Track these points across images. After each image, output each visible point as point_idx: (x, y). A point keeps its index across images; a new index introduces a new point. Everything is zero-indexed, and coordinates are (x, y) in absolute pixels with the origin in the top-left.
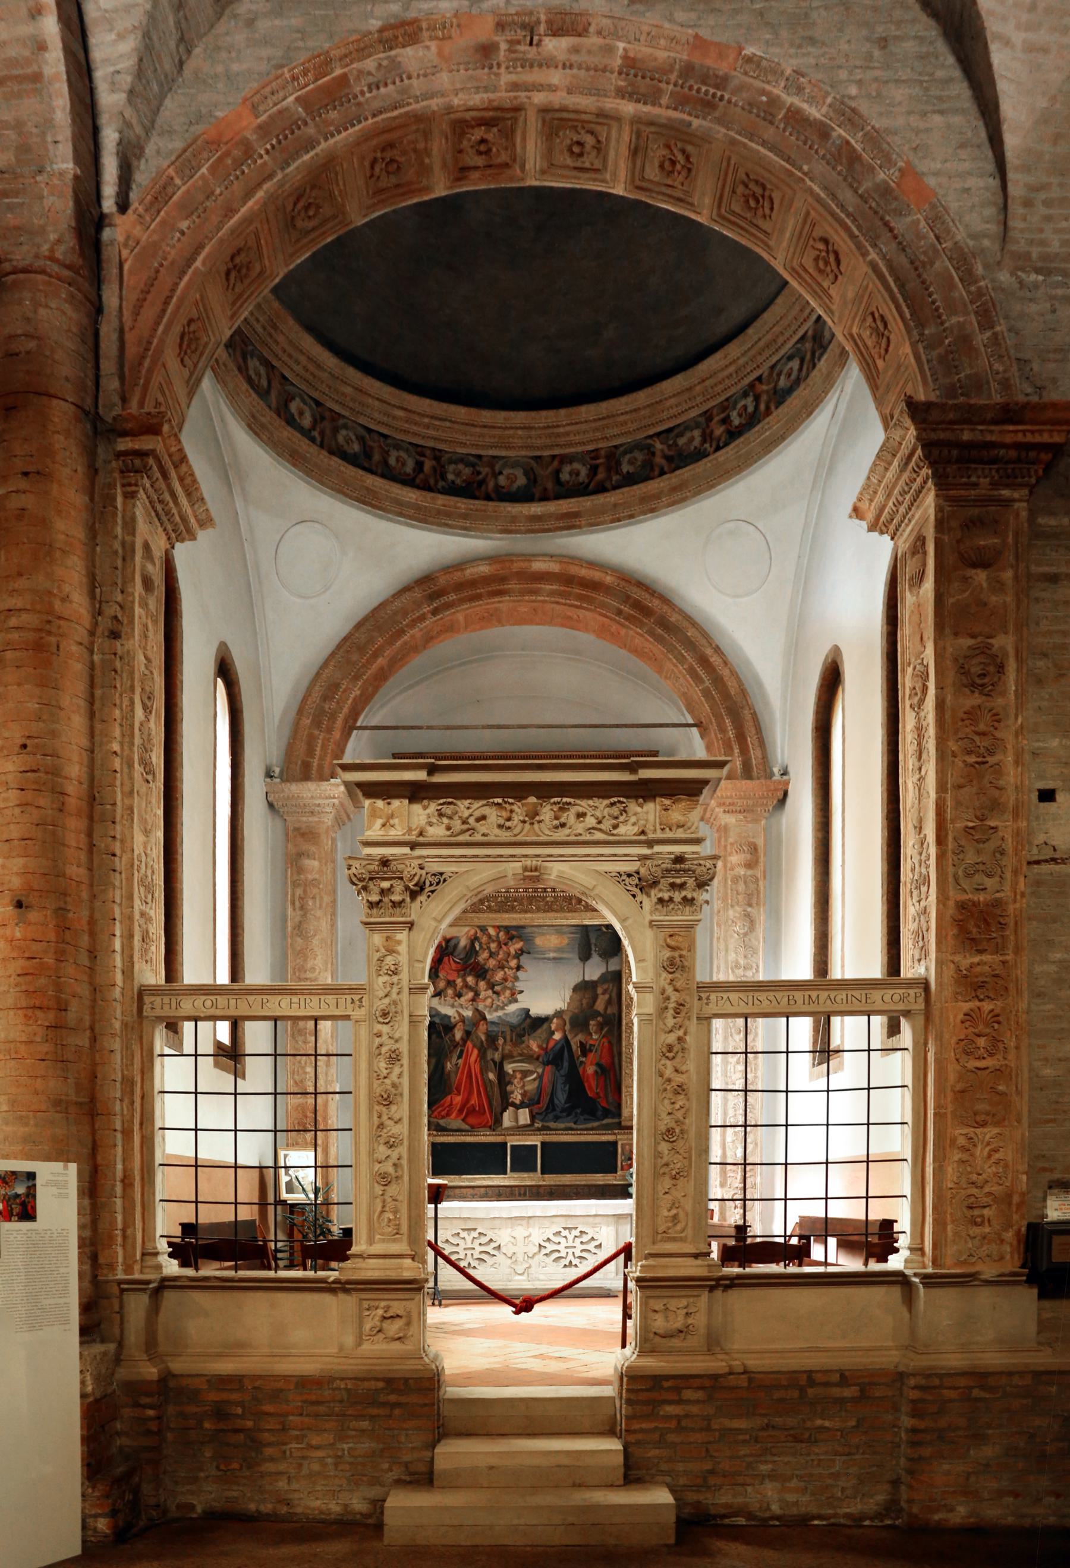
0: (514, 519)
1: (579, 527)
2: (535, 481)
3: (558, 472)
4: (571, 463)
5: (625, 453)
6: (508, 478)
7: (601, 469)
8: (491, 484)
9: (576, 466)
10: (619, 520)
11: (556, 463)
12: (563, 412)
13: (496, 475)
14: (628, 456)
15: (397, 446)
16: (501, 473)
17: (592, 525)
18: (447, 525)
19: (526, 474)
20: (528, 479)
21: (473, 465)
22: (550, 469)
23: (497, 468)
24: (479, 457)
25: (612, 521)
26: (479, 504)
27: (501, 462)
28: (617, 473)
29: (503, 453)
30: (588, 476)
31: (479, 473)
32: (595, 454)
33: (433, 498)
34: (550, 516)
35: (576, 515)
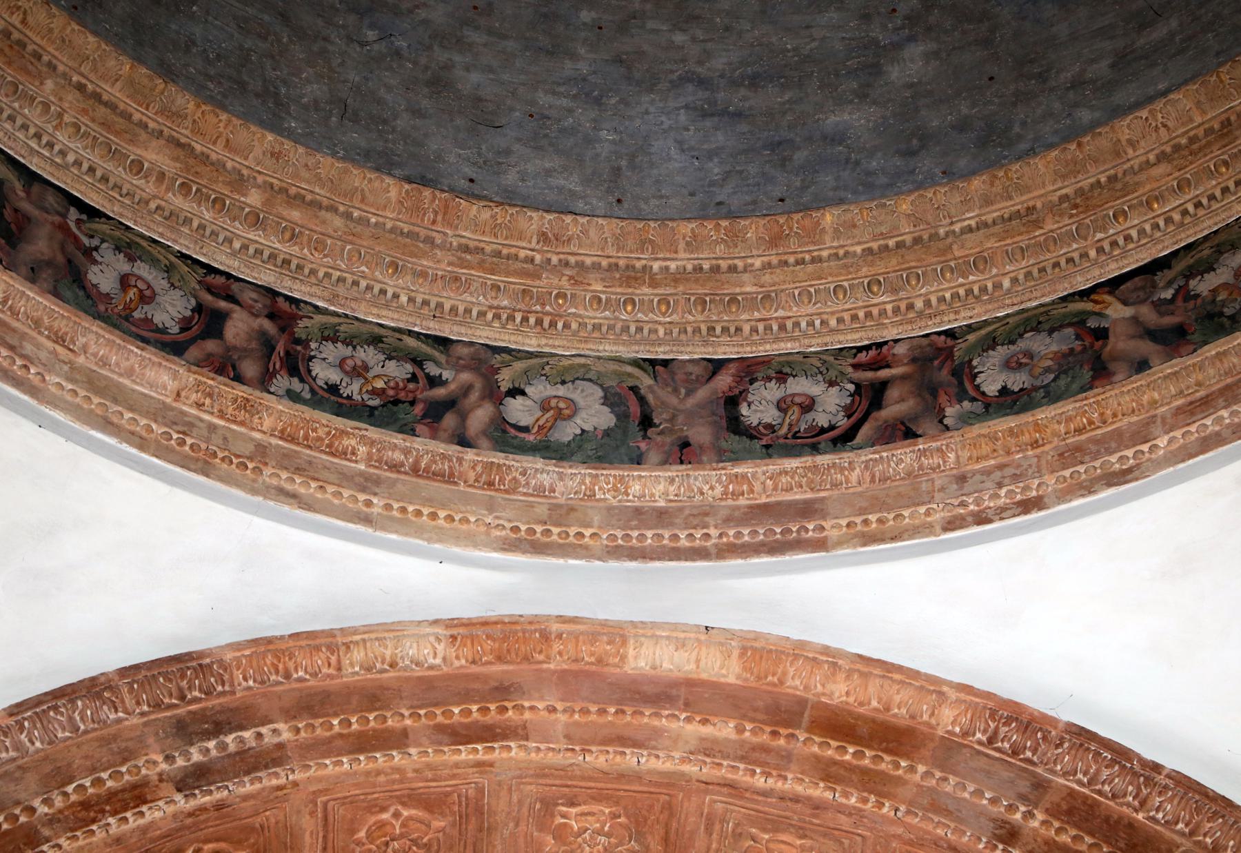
0: (562, 514)
1: (820, 545)
2: (646, 422)
3: (732, 402)
4: (782, 377)
5: (991, 343)
6: (545, 406)
7: (893, 393)
8: (480, 416)
9: (800, 386)
10: (981, 519)
11: (724, 381)
12: (753, 229)
13: (496, 396)
14: (1002, 352)
15: (131, 246)
16: (516, 392)
17: (870, 539)
18: (292, 497)
19: (611, 400)
20: (622, 417)
21: (418, 361)
22: (702, 393)
23: (505, 379)
24: (443, 343)
25: (951, 525)
26: (424, 447)
27: (519, 366)
28: (962, 396)
29: (531, 343)
30: (849, 411)
31: (434, 382)
32: (877, 356)
33: (245, 405)
34: (701, 516)
35: (807, 510)
